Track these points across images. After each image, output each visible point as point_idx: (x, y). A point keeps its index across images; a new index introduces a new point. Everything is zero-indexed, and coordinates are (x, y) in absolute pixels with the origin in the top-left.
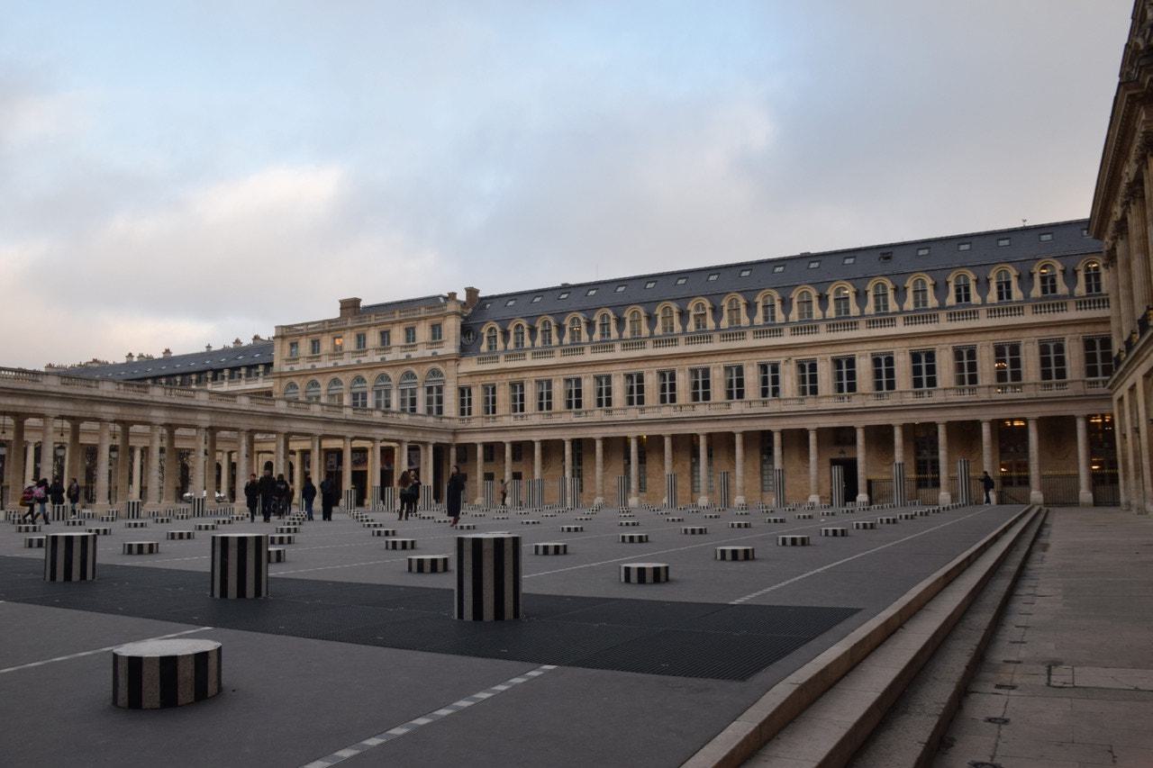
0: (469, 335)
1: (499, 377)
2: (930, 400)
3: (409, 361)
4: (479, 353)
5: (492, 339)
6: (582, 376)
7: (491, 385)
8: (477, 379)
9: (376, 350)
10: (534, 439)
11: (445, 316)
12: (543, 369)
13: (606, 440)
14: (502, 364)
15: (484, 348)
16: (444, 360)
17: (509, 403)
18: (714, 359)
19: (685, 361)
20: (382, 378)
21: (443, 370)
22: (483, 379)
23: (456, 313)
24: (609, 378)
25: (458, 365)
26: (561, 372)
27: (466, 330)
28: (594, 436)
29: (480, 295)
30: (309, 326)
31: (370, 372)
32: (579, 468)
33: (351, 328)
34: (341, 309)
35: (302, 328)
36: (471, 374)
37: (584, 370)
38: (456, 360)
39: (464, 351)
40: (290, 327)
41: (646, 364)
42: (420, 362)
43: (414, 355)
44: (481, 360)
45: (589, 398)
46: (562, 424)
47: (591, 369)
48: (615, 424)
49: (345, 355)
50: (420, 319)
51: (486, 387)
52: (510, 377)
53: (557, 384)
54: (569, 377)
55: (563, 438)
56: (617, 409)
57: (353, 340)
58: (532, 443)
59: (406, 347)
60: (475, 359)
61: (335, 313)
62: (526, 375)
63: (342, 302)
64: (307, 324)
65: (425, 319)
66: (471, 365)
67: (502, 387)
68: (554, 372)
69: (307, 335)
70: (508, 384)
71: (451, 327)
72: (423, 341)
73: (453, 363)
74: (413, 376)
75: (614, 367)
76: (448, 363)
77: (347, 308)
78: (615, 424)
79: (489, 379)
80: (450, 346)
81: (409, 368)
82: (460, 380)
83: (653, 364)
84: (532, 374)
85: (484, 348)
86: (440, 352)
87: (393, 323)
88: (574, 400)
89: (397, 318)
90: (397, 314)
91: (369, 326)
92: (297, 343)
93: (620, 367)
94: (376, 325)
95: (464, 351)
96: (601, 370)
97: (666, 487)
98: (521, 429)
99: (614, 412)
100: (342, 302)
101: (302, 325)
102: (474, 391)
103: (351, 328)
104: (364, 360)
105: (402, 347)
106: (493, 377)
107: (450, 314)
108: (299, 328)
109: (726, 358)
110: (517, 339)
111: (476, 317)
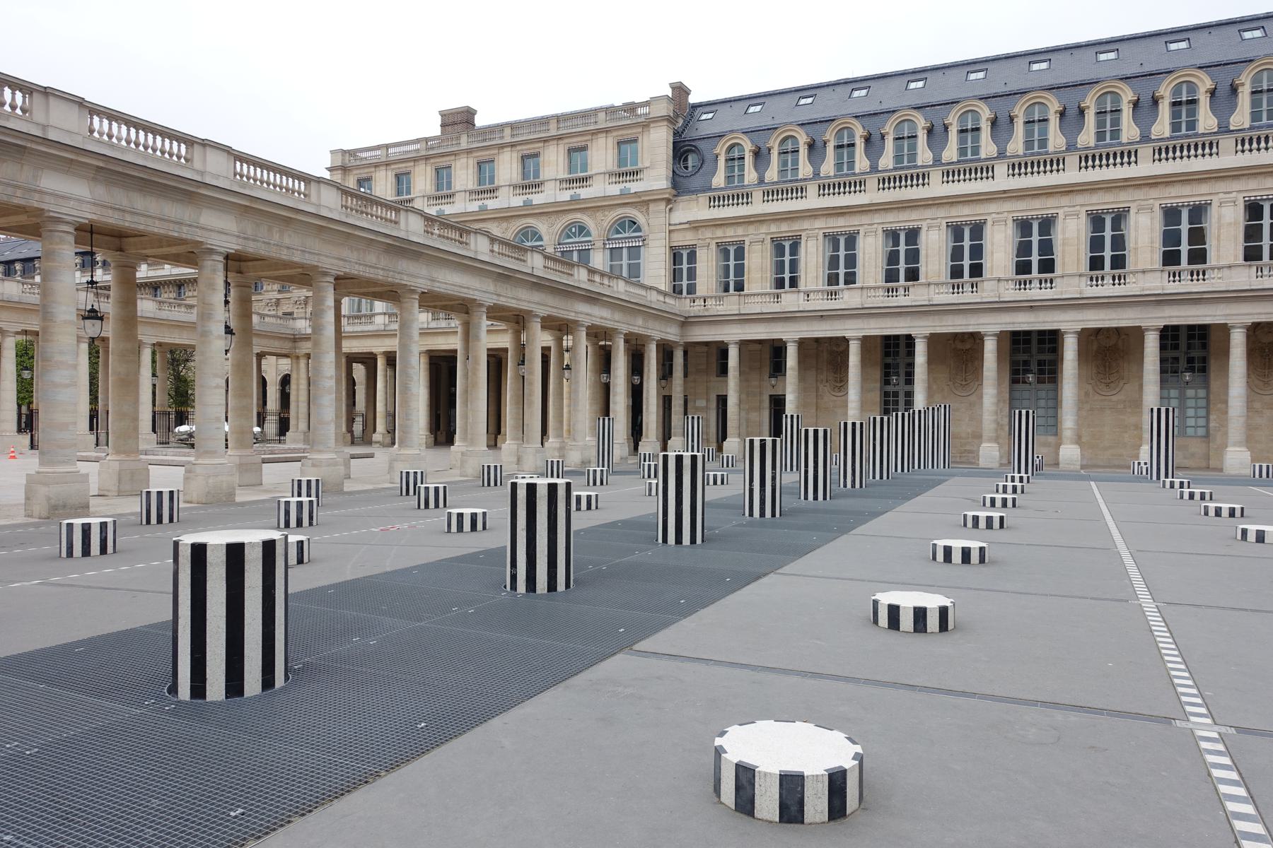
0: (686, 160)
1: (751, 229)
3: (577, 205)
4: (710, 189)
5: (735, 161)
6: (924, 225)
7: (732, 243)
8: (708, 234)
9: (515, 187)
11: (646, 125)
14: (758, 206)
15: (719, 180)
16: (644, 201)
17: (769, 275)
18: (1221, 186)
19: (1154, 193)
20: (525, 235)
21: (641, 219)
22: (719, 233)
23: (662, 118)
25: (671, 210)
26: (878, 218)
27: (682, 150)
28: (982, 329)
29: (693, 99)
30: (391, 151)
31: (505, 225)
32: (907, 388)
33: (469, 151)
34: (443, 126)
35: (378, 152)
36: (695, 226)
37: (928, 213)
38: (668, 201)
39: (679, 186)
40: (352, 153)
41: (1065, 200)
42: (596, 207)
43: (584, 193)
44: (716, 201)
46: (864, 308)
47: (941, 212)
49: (458, 197)
50: (595, 133)
51: (723, 250)
52: (773, 228)
53: (870, 240)
54: (894, 226)
55: (913, 332)
56: (1213, 269)
57: (471, 171)
58: (845, 341)
59: (571, 181)
60: (703, 199)
61: (437, 131)
62: (806, 224)
63: (443, 114)
64: (387, 146)
65: (606, 131)
66: (694, 209)
67: (758, 247)
68: (865, 219)
69: (387, 164)
70: (768, 241)
71: (657, 144)
72: (603, 170)
73: (662, 206)
74: (582, 229)
76: (652, 207)
77: (454, 124)
79: (731, 234)
80: (657, 178)
81: (579, 216)
82: (675, 236)
83: (1080, 199)
84: (819, 223)
85: (719, 180)
86: (634, 187)
87: (545, 141)
89: (553, 132)
90: (553, 125)
91: (502, 147)
92: (369, 179)
94: (513, 145)
95: (679, 186)
96: (964, 214)
97: (1147, 427)
98: (822, 316)
100: (443, 114)
101: (378, 147)
102: (701, 255)
103: (469, 151)
104: (492, 204)
105: (561, 181)
106: (740, 231)
107: (656, 120)
108: (364, 155)
109: (1252, 184)
110: (785, 163)
111: (690, 136)
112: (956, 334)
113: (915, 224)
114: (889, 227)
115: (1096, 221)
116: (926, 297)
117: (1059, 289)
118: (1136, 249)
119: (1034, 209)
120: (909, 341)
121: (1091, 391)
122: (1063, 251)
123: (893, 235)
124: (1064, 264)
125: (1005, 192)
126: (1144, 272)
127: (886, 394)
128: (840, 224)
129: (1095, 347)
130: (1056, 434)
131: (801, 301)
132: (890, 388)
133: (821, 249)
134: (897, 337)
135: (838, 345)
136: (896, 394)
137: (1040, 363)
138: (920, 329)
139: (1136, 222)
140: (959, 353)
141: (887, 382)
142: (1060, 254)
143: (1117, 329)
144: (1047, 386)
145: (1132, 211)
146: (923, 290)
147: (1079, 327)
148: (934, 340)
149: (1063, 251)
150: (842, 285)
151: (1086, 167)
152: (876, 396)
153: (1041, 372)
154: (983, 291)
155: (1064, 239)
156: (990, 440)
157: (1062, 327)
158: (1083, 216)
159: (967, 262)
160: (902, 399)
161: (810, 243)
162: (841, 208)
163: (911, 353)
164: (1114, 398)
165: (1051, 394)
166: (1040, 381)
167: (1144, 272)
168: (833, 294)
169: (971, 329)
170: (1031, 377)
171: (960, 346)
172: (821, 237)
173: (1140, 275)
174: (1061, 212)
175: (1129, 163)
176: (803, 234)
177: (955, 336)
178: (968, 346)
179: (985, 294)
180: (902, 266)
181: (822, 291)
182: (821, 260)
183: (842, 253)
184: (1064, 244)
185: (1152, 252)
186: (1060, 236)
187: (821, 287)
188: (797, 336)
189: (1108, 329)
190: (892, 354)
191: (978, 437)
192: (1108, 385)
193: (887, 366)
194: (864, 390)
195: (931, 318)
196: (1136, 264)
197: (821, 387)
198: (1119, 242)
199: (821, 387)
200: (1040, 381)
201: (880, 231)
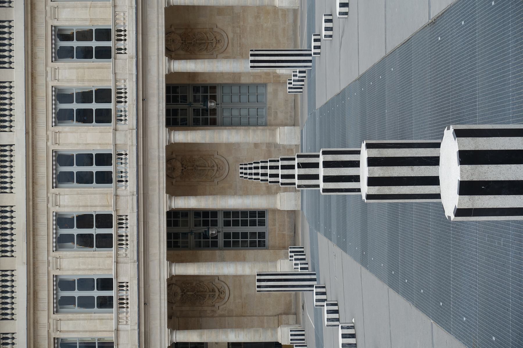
2: (132, 221)
6: (54, 209)
10: (165, 276)
12: (35, 293)
13: (173, 121)
24: (62, 159)
37: (42, 206)
41: (41, 81)
45: (90, 199)
47: (42, 193)
48: (143, 100)
53: (65, 263)
54: (52, 240)
55: (164, 210)
68: (43, 269)
75: (41, 145)
78: (143, 100)
83: (40, 68)
84: (43, 318)
88: (96, 169)
93: (41, 131)
96: (45, 171)
98: (145, 303)
99: (121, 85)
112: (168, 176)
113: (52, 218)
114: (52, 245)
115: (63, 54)
116: (129, 198)
117: (127, 77)
118: (91, 20)
119: (46, 107)
120: (174, 217)
121: (223, 55)
122: (89, 81)
123: (62, 241)
124: (101, 80)
125: (27, 133)
126: (115, 6)
127: (227, 245)
128: (46, 295)
129: (182, 52)
130: (265, 85)
131: (128, 328)
132: (221, 240)
133: (70, 316)
134: (169, 235)
135: (175, 294)
136: (227, 235)
137: (196, 100)
138: (161, 203)
139: (67, 20)
140: (185, 169)
141: (215, 245)
142: (92, 84)
143: (166, 34)
144: (219, 93)
145: (56, 23)
146: (122, 201)
147: (164, 59)
148: (173, 190)
149: (89, 81)
150: (113, 293)
151: (10, 63)
152: (230, 253)
153: (205, 100)
154: (125, 145)
155: (78, 81)
156: (274, 135)
157: (163, 72)
158: (57, 64)
159: (96, 169)
160: (232, 229)
161: (64, 327)
162: (28, 294)
163: (185, 213)
164: (231, 35)
165: (227, 90)
166: (214, 98)
167: (115, 6)
168: (122, 302)
169: (163, 155)
170: (211, 105)
171: (178, 172)
172: (58, 316)
173: (118, 9)
174: (51, 84)
175: (10, 27)
176: (53, 335)
177: (169, 177)
178: (179, 164)
179: (129, 143)
180: (94, 231)
181: (118, 313)
182: (82, 316)
183: (77, 294)
184: (83, 80)
185: (95, 7)
186: (75, 84)
187: (114, 315)
188: (166, 331)
189: (167, 41)
190: (188, 234)
191: (271, 146)
192: (218, 42)
193: (199, 246)
194: (223, 260)
195: (150, 193)
196: (105, 19)
197: (219, 312)
198: (85, 35)
199: (219, 312)
200: (214, 98)
201: (57, 254)
